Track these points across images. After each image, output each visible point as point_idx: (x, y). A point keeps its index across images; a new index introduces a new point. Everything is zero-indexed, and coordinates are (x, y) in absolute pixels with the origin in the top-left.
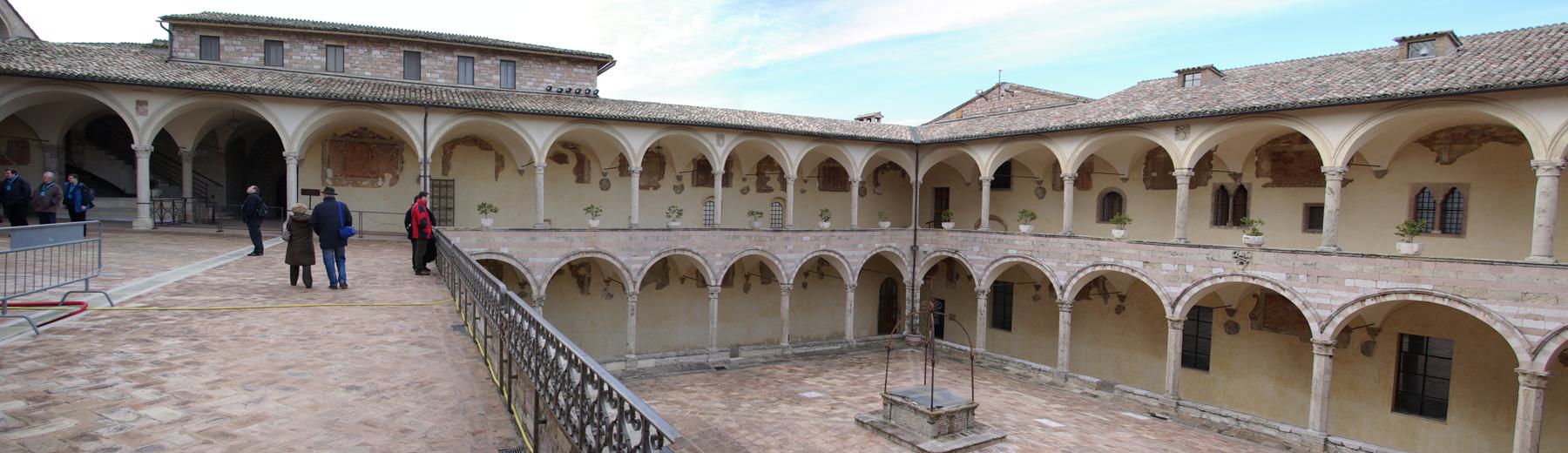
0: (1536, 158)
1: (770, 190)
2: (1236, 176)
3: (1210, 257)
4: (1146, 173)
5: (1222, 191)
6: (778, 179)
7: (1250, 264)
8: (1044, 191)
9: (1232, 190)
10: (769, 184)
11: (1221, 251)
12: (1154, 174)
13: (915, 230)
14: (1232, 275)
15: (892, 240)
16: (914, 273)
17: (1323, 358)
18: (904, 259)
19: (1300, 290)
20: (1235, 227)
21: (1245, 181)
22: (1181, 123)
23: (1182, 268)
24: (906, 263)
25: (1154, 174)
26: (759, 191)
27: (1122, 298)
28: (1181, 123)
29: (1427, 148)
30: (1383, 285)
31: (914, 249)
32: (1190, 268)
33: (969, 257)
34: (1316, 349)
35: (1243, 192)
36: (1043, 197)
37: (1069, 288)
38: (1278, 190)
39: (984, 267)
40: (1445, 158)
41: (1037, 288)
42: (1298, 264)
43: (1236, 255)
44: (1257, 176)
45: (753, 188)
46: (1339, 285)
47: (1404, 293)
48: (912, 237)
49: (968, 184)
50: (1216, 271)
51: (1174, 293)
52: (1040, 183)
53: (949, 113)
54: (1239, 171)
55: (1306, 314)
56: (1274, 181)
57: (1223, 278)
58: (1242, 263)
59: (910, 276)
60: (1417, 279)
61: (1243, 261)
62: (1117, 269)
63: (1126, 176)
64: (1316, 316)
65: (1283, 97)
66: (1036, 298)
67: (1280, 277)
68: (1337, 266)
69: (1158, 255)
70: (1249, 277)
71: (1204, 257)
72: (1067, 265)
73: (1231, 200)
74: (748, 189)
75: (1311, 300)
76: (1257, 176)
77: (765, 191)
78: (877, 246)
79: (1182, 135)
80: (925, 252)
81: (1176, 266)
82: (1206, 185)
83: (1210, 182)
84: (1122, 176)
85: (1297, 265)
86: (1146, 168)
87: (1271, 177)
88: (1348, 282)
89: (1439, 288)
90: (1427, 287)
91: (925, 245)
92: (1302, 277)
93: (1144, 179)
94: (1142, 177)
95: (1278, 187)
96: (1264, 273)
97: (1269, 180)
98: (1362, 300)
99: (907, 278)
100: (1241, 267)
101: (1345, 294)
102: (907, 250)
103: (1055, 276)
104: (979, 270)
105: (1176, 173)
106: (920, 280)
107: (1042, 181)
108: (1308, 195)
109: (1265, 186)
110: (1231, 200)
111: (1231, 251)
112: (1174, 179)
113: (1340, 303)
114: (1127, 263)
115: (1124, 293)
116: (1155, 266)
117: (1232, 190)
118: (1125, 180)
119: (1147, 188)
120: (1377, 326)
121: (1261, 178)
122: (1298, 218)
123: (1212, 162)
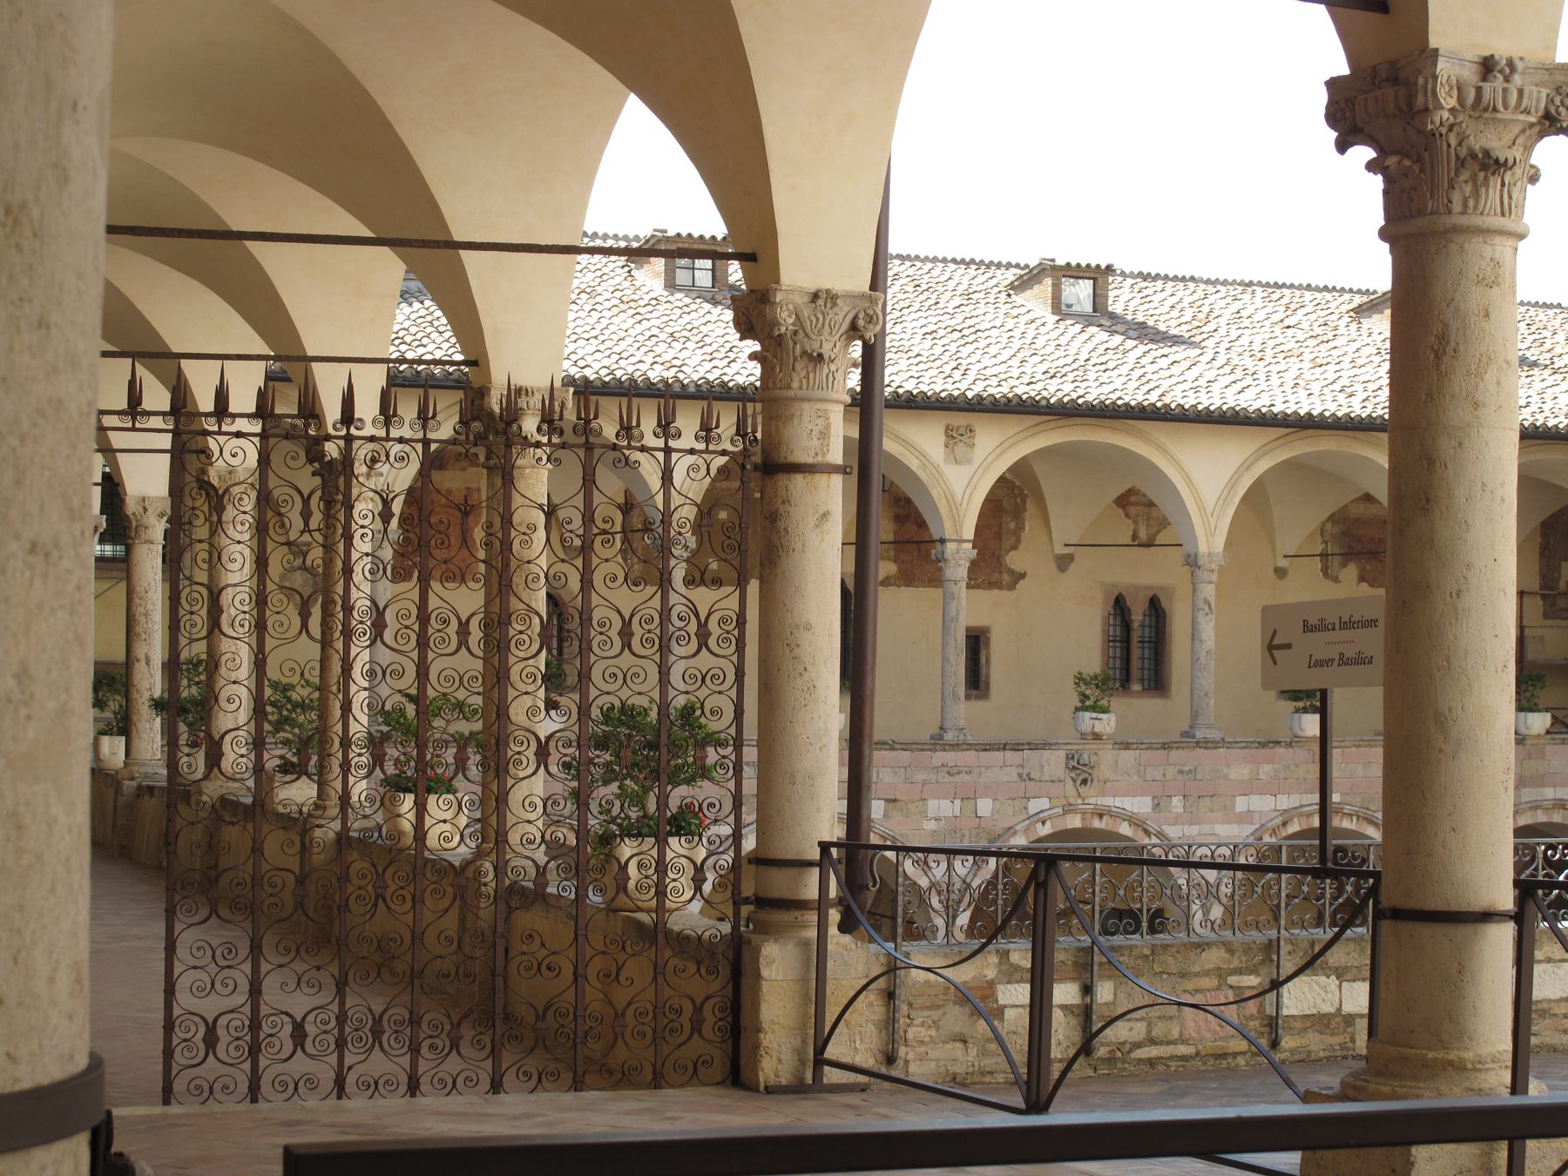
3: (1025, 772)
7: (1095, 781)
11: (1046, 753)
14: (1065, 812)
23: (969, 805)
29: (1121, 510)
30: (1285, 802)
32: (985, 806)
42: (1171, 772)
50: (1035, 806)
56: (900, 571)
57: (1048, 823)
58: (1084, 782)
61: (1081, 772)
67: (1139, 805)
68: (1225, 771)
69: (920, 777)
71: (1012, 774)
79: (960, 449)
81: (958, 802)
85: (1168, 777)
87: (895, 561)
88: (1241, 804)
89: (1348, 799)
92: (1177, 802)
95: (908, 586)
96: (1118, 802)
100: (1082, 790)
111: (1062, 754)
116: (912, 807)
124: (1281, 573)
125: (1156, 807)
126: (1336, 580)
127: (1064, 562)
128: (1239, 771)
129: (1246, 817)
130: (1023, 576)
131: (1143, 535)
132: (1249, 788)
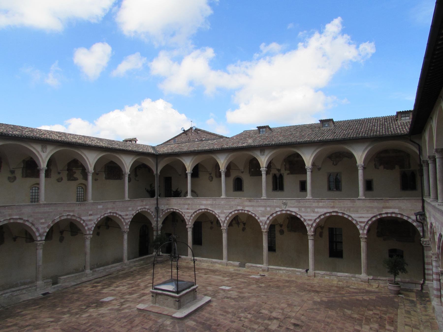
0: (358, 163)
1: (76, 179)
2: (279, 170)
4: (250, 170)
6: (81, 173)
8: (212, 178)
9: (278, 176)
10: (75, 176)
12: (252, 170)
13: (157, 199)
15: (146, 205)
16: (157, 221)
17: (311, 240)
18: (152, 214)
19: (302, 214)
20: (280, 191)
22: (262, 148)
24: (153, 217)
25: (252, 170)
26: (69, 179)
27: (244, 224)
28: (262, 148)
30: (325, 210)
31: (157, 209)
33: (183, 211)
35: (281, 177)
36: (212, 180)
37: (226, 222)
38: (291, 176)
39: (190, 215)
40: (335, 163)
41: (212, 223)
43: (283, 202)
44: (285, 170)
45: (65, 178)
46: (314, 212)
48: (155, 202)
49: (180, 175)
51: (264, 220)
52: (210, 174)
53: (170, 140)
54: (279, 168)
55: (305, 224)
59: (156, 223)
60: (333, 207)
62: (243, 211)
63: (243, 171)
64: (308, 225)
65: (292, 140)
66: (211, 228)
70: (287, 210)
72: (225, 211)
74: (62, 179)
75: (305, 218)
76: (285, 170)
77: (73, 180)
78: (139, 208)
79: (262, 153)
80: (163, 210)
83: (271, 173)
84: (241, 171)
86: (249, 167)
88: (316, 210)
90: (336, 210)
91: (163, 206)
93: (249, 172)
94: (248, 171)
95: (292, 174)
97: (289, 172)
98: (320, 216)
99: (154, 224)
101: (315, 215)
102: (153, 209)
103: (219, 217)
104: (188, 217)
105: (261, 169)
106: (160, 225)
107: (211, 173)
108: (300, 178)
109: (288, 174)
112: (261, 171)
113: (314, 218)
114: (247, 209)
115: (245, 222)
117: (278, 176)
118: (242, 172)
119: (251, 176)
120: (323, 226)
121: (286, 171)
122: (298, 187)
123: (271, 165)
125: (299, 210)
126: (378, 169)
128: (315, 204)
129: (317, 212)
131: (335, 163)
132: (317, 207)
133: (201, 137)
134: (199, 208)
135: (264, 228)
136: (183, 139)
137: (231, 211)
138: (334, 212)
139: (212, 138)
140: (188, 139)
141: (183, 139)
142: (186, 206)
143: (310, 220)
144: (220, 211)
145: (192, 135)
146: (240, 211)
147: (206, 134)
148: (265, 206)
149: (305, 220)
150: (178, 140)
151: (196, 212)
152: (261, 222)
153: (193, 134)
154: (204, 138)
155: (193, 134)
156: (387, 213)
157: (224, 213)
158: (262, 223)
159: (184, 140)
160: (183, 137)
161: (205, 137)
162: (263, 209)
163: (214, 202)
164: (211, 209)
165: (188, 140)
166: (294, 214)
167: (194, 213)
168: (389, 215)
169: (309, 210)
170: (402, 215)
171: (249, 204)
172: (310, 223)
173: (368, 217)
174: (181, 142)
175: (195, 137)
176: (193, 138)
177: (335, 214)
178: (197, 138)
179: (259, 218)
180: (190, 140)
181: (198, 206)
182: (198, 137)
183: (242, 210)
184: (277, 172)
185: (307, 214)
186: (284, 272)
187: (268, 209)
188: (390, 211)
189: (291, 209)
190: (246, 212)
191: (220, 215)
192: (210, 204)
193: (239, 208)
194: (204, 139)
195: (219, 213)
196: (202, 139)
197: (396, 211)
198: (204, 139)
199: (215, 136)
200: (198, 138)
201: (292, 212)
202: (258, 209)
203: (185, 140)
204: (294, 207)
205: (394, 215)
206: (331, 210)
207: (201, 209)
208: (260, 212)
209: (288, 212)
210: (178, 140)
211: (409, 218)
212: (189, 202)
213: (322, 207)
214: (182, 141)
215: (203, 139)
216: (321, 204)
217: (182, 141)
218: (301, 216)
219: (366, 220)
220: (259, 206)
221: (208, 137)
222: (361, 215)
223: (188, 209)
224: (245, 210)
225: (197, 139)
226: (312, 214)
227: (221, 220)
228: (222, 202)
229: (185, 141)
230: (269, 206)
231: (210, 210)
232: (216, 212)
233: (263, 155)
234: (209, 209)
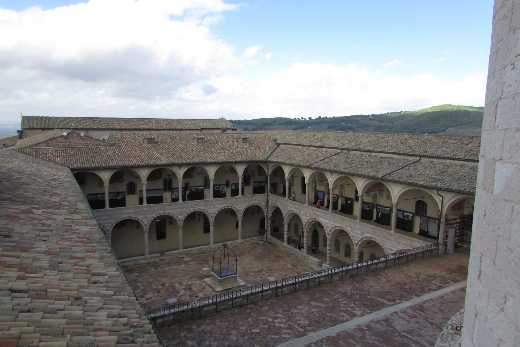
2: (169, 175)
5: (165, 180)
9: (168, 180)
19: (208, 210)
21: (171, 177)
34: (211, 224)
46: (215, 208)
47: (224, 207)
60: (226, 203)
62: (164, 214)
72: (148, 216)
73: (168, 183)
75: (210, 212)
82: (161, 179)
88: (216, 206)
90: (228, 205)
98: (218, 210)
104: (108, 226)
110: (168, 183)
113: (215, 212)
114: (167, 211)
117: (168, 180)
124: (226, 173)
127: (198, 174)
128: (215, 203)
129: (217, 208)
130: (193, 176)
132: (217, 204)
133: (86, 143)
134: (121, 217)
135: (181, 224)
136: (61, 143)
137: (154, 215)
138: (227, 206)
139: (101, 145)
140: (67, 143)
141: (61, 143)
142: (105, 218)
143: (212, 213)
144: (142, 217)
145: (73, 140)
146: (162, 214)
147: (93, 140)
148: (182, 208)
149: (209, 214)
150: (52, 144)
151: (117, 221)
152: (179, 220)
153: (75, 139)
154: (91, 144)
155: (75, 139)
156: (252, 204)
157: (147, 218)
158: (180, 221)
159: (62, 145)
160: (59, 141)
161: (92, 143)
162: (180, 210)
163: (137, 210)
164: (134, 216)
165: (68, 144)
166: (202, 211)
167: (115, 222)
168: (253, 204)
169: (212, 207)
170: (259, 203)
171: (169, 207)
172: (212, 215)
173: (243, 207)
174: (58, 146)
175: (78, 143)
176: (75, 143)
177: (226, 207)
178: (81, 144)
179: (177, 217)
180: (70, 145)
181: (119, 215)
182: (82, 143)
183: (163, 213)
184: (167, 177)
185: (211, 210)
186: (195, 251)
187: (184, 210)
188: (254, 202)
189: (201, 208)
190: (167, 214)
191: (143, 220)
192: (132, 213)
193: (161, 212)
194: (92, 145)
195: (141, 218)
196: (88, 146)
197: (256, 202)
198: (92, 145)
199: (105, 143)
200: (83, 144)
201: (201, 209)
202: (176, 210)
203: (64, 144)
204: (204, 206)
205: (255, 204)
206: (224, 205)
207: (123, 218)
208: (178, 212)
209: (199, 210)
210: (52, 144)
211: (262, 204)
212: (108, 213)
213: (220, 204)
214: (59, 145)
215: (90, 145)
216: (219, 202)
217: (60, 146)
218: (207, 212)
219: (242, 209)
220: (177, 209)
221: (96, 144)
222: (240, 206)
223: (107, 220)
224: (165, 213)
225: (82, 145)
226: (214, 209)
227: (144, 224)
228: (145, 209)
229: (63, 146)
230: (185, 208)
231: (133, 217)
232: (139, 218)
233: (181, 170)
234: (132, 216)
